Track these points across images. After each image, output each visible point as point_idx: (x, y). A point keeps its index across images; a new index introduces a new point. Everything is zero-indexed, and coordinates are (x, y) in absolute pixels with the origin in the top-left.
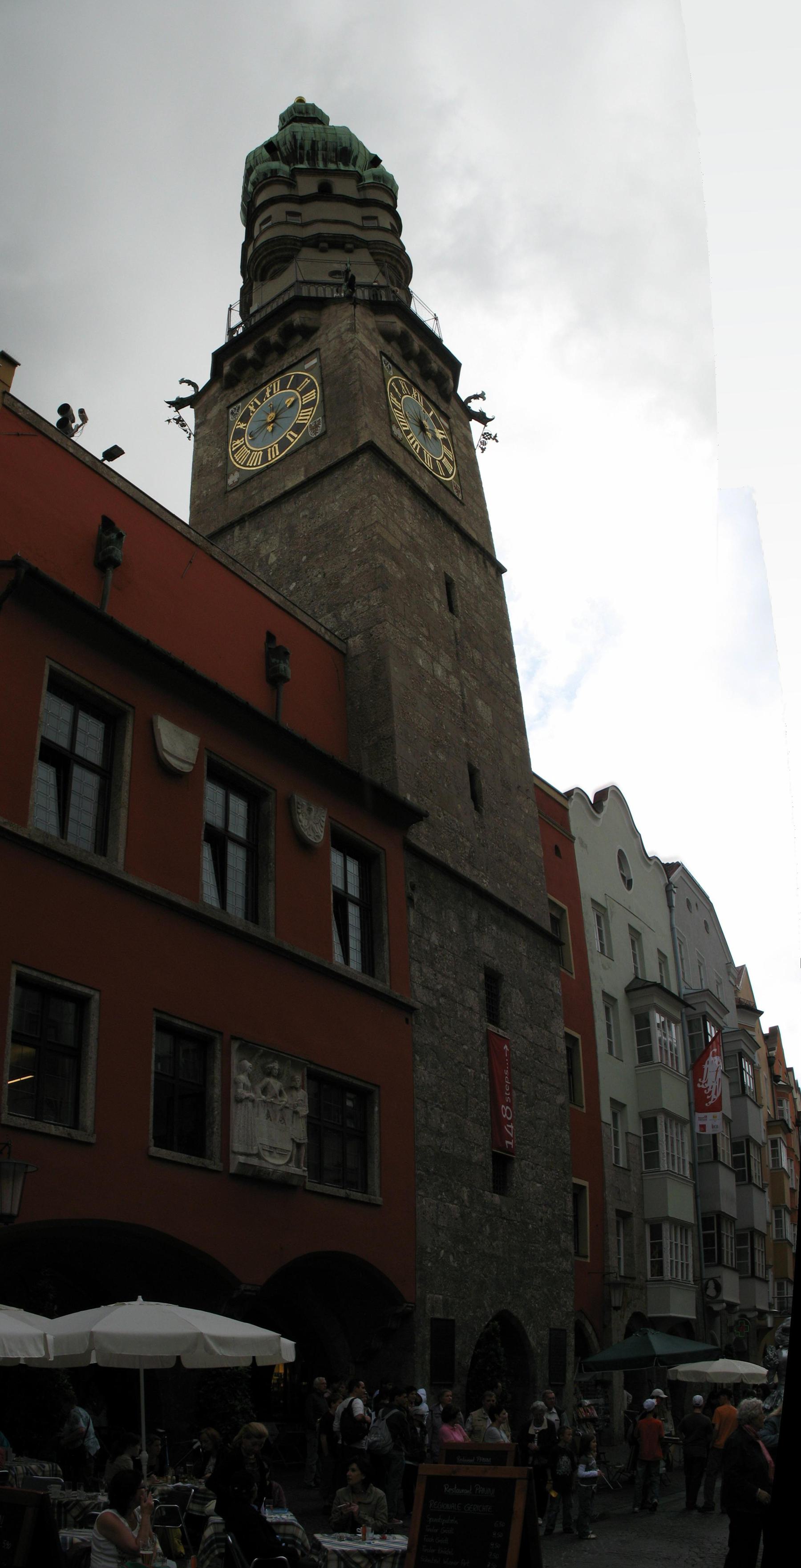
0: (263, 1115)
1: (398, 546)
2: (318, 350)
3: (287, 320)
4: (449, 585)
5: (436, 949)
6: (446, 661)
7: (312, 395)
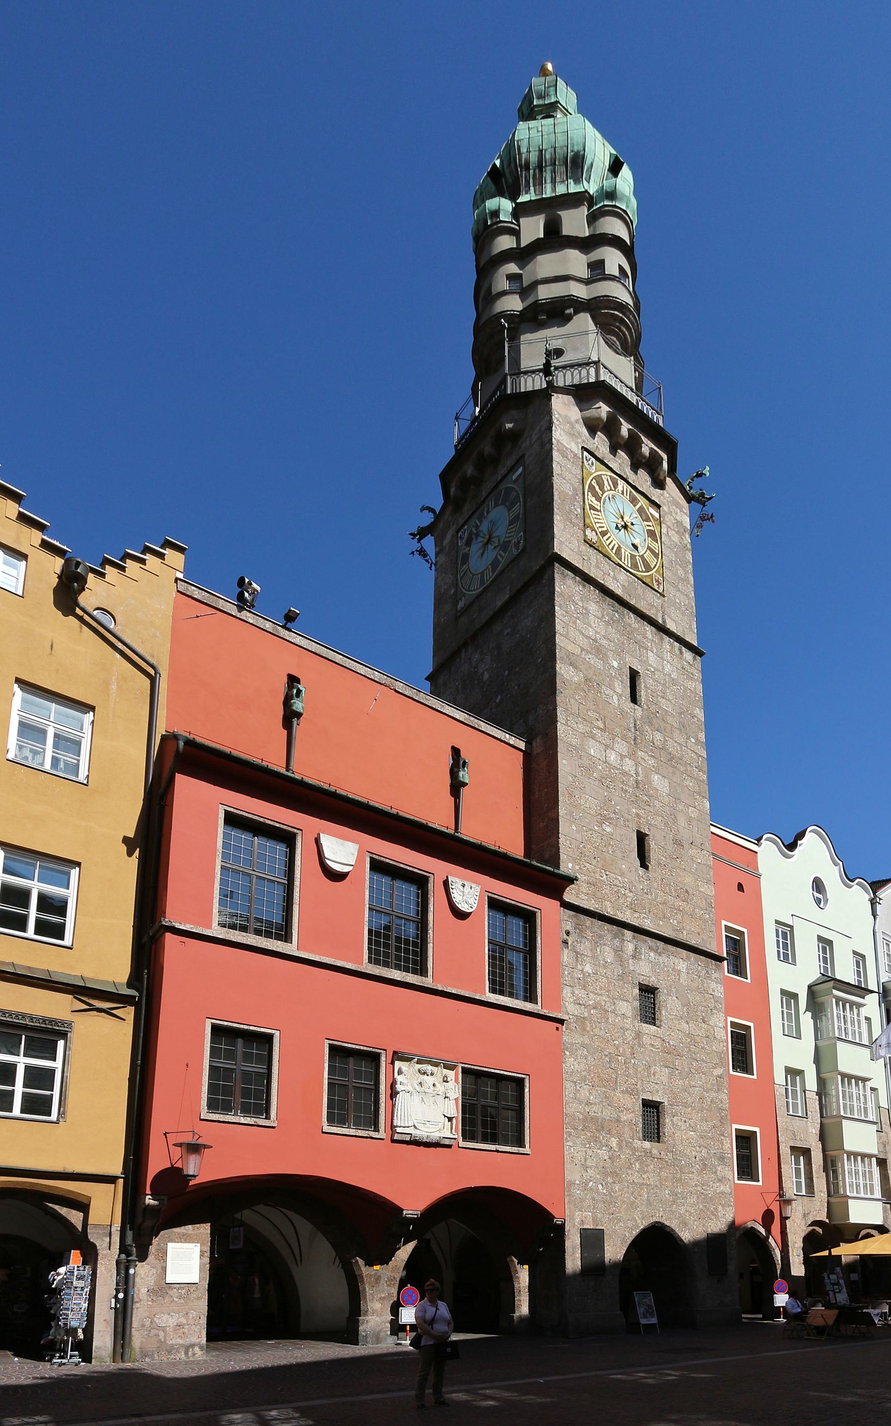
1: (577, 651)
2: (523, 456)
4: (634, 676)
5: (589, 975)
6: (621, 746)
7: (518, 509)
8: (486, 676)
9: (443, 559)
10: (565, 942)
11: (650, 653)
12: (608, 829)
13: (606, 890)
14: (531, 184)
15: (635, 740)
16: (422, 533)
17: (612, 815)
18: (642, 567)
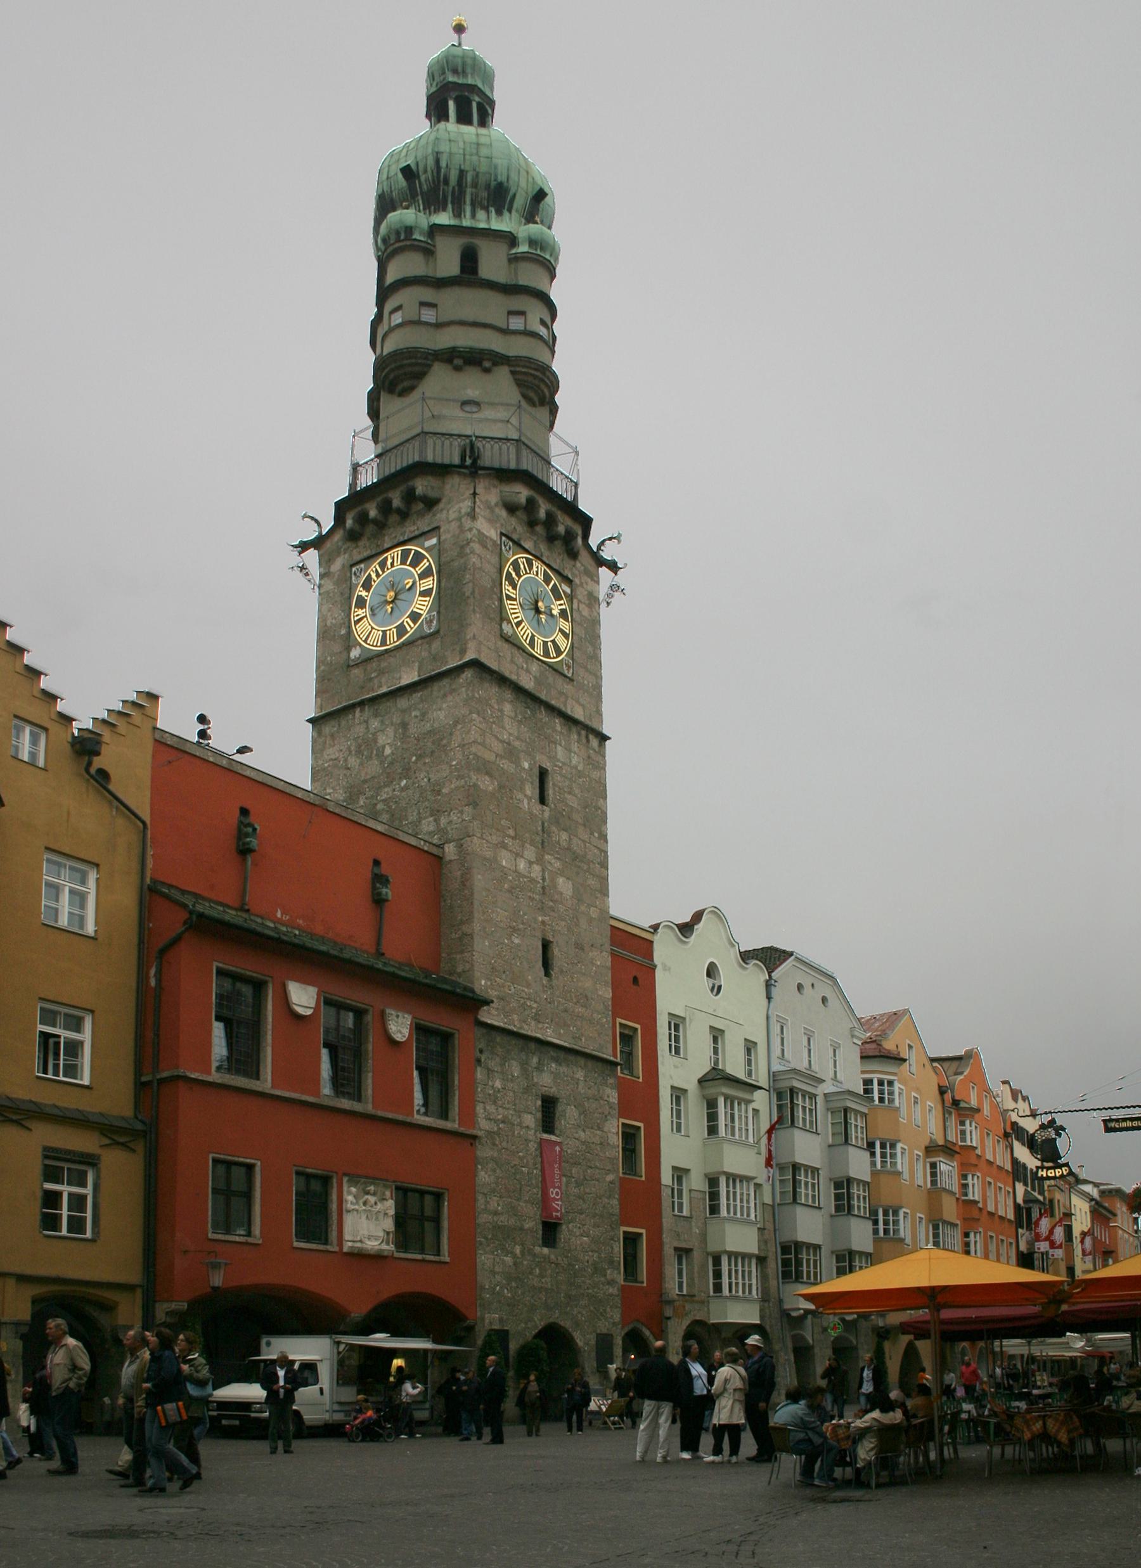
0: (364, 1217)
3: (410, 483)
4: (543, 774)
6: (530, 853)
8: (388, 751)
9: (329, 585)
10: (479, 1061)
11: (559, 748)
12: (517, 941)
13: (514, 1004)
14: (450, 199)
15: (543, 842)
16: (304, 547)
17: (521, 926)
18: (553, 653)
